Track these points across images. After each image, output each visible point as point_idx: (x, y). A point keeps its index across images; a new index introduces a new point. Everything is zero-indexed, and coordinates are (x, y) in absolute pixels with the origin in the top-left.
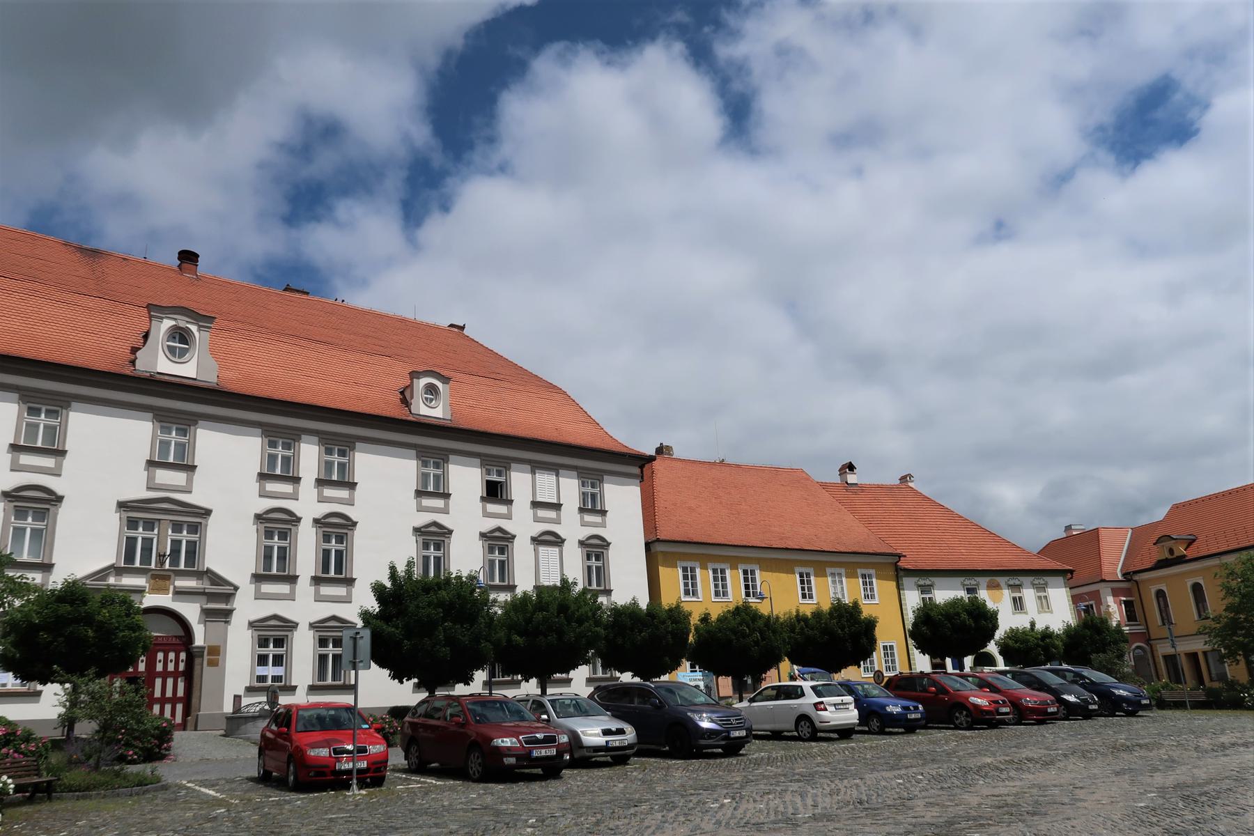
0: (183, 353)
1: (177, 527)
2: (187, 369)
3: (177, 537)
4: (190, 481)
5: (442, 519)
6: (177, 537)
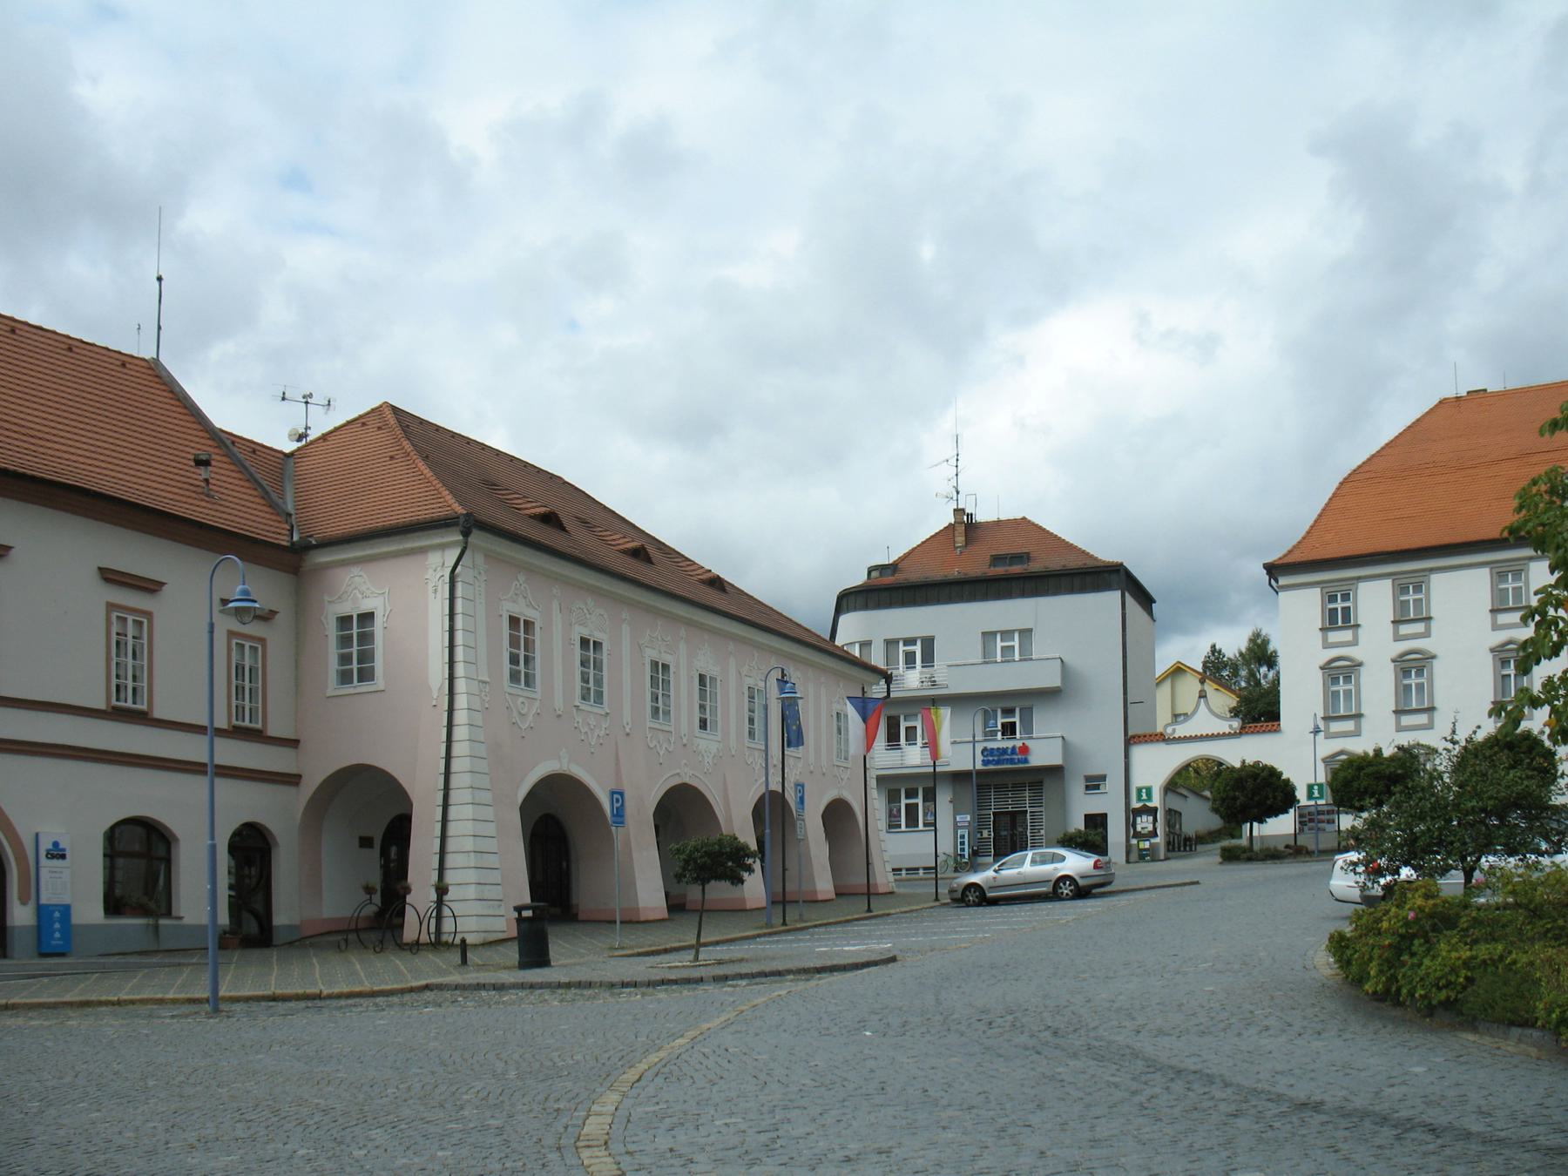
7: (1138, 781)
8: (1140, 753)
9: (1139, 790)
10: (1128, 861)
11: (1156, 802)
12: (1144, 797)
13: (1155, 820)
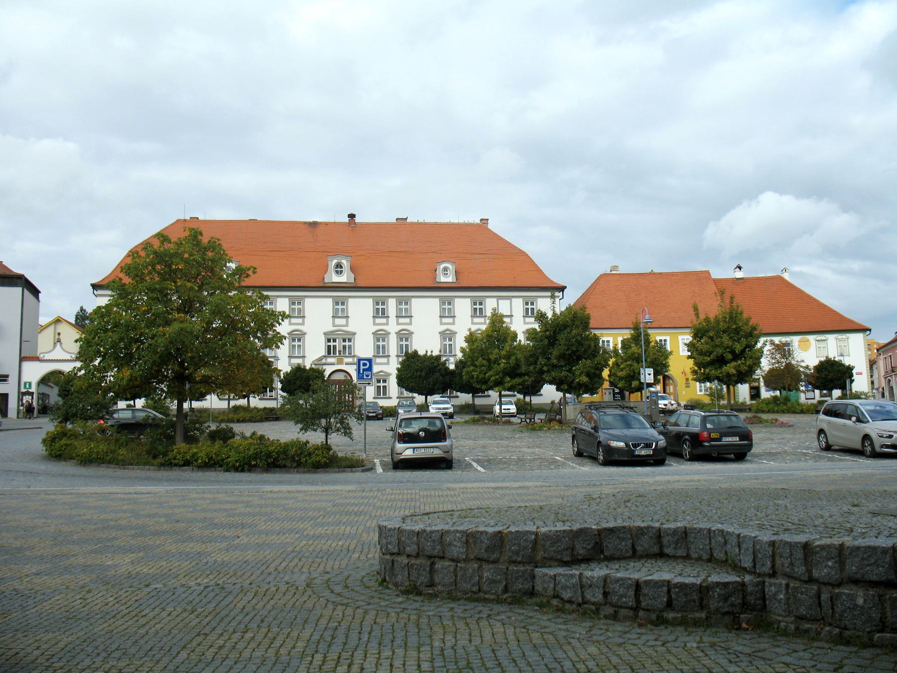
0: (341, 272)
1: (344, 340)
2: (343, 278)
3: (344, 344)
4: (347, 322)
5: (451, 327)
6: (344, 344)
7: (25, 379)
8: (26, 365)
9: (25, 383)
10: (18, 418)
11: (33, 389)
12: (28, 387)
13: (32, 398)
